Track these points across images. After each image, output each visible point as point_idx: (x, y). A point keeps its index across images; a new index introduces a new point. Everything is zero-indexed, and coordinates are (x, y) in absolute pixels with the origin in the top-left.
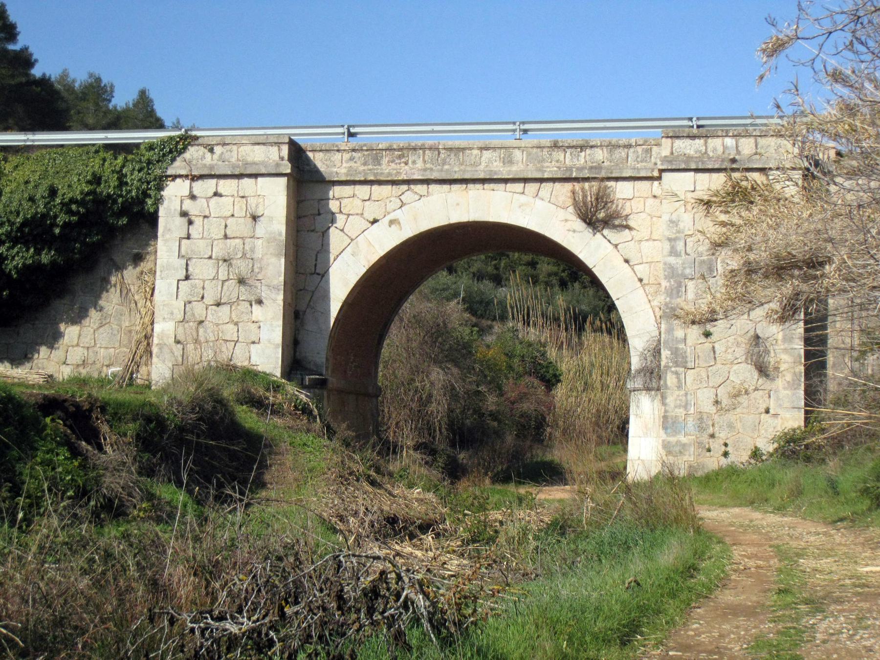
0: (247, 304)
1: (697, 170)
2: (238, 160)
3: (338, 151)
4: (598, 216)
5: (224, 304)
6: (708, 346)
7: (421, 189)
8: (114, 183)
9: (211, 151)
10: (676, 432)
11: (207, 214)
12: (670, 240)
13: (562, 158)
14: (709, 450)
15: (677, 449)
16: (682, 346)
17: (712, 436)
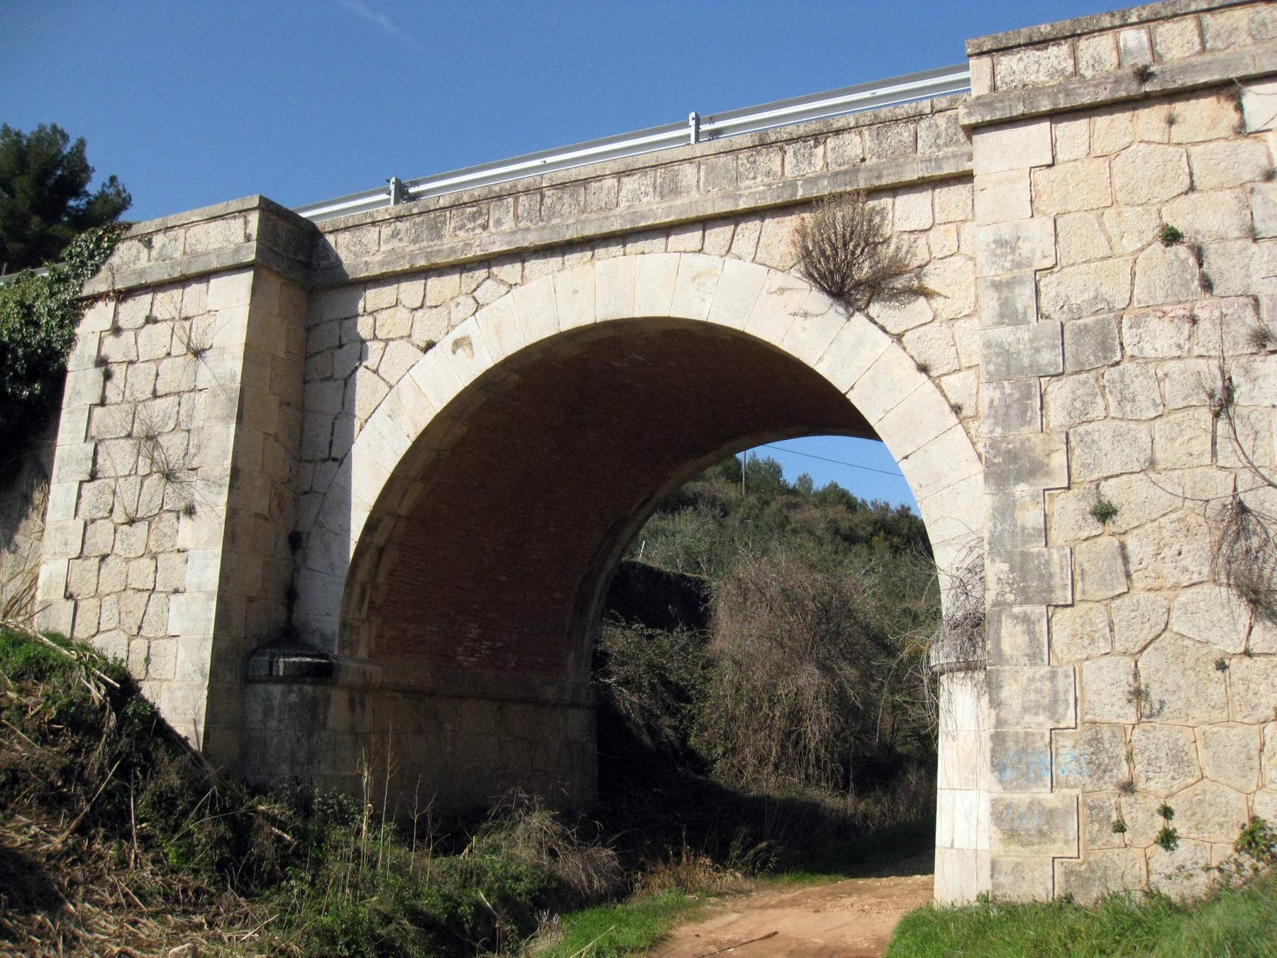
0: (173, 515)
1: (1056, 115)
2: (185, 253)
3: (373, 223)
4: (852, 274)
5: (142, 519)
6: (1108, 543)
7: (509, 271)
9: (149, 245)
10: (1028, 778)
11: (133, 357)
12: (997, 286)
13: (776, 166)
14: (1120, 828)
15: (1032, 824)
16: (1036, 547)
17: (1128, 788)
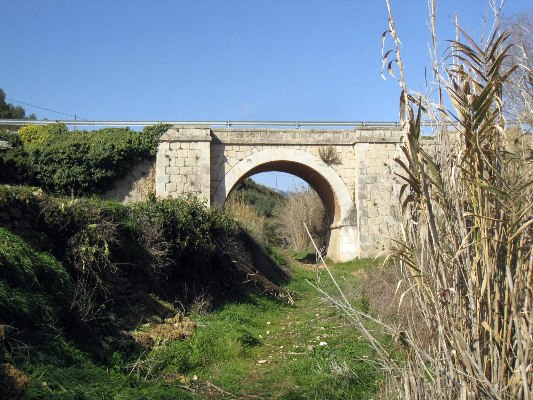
1: (370, 143)
4: (330, 159)
6: (375, 209)
7: (260, 147)
8: (137, 143)
9: (178, 131)
10: (365, 241)
12: (360, 169)
14: (377, 248)
15: (365, 248)
16: (366, 209)
17: (378, 243)
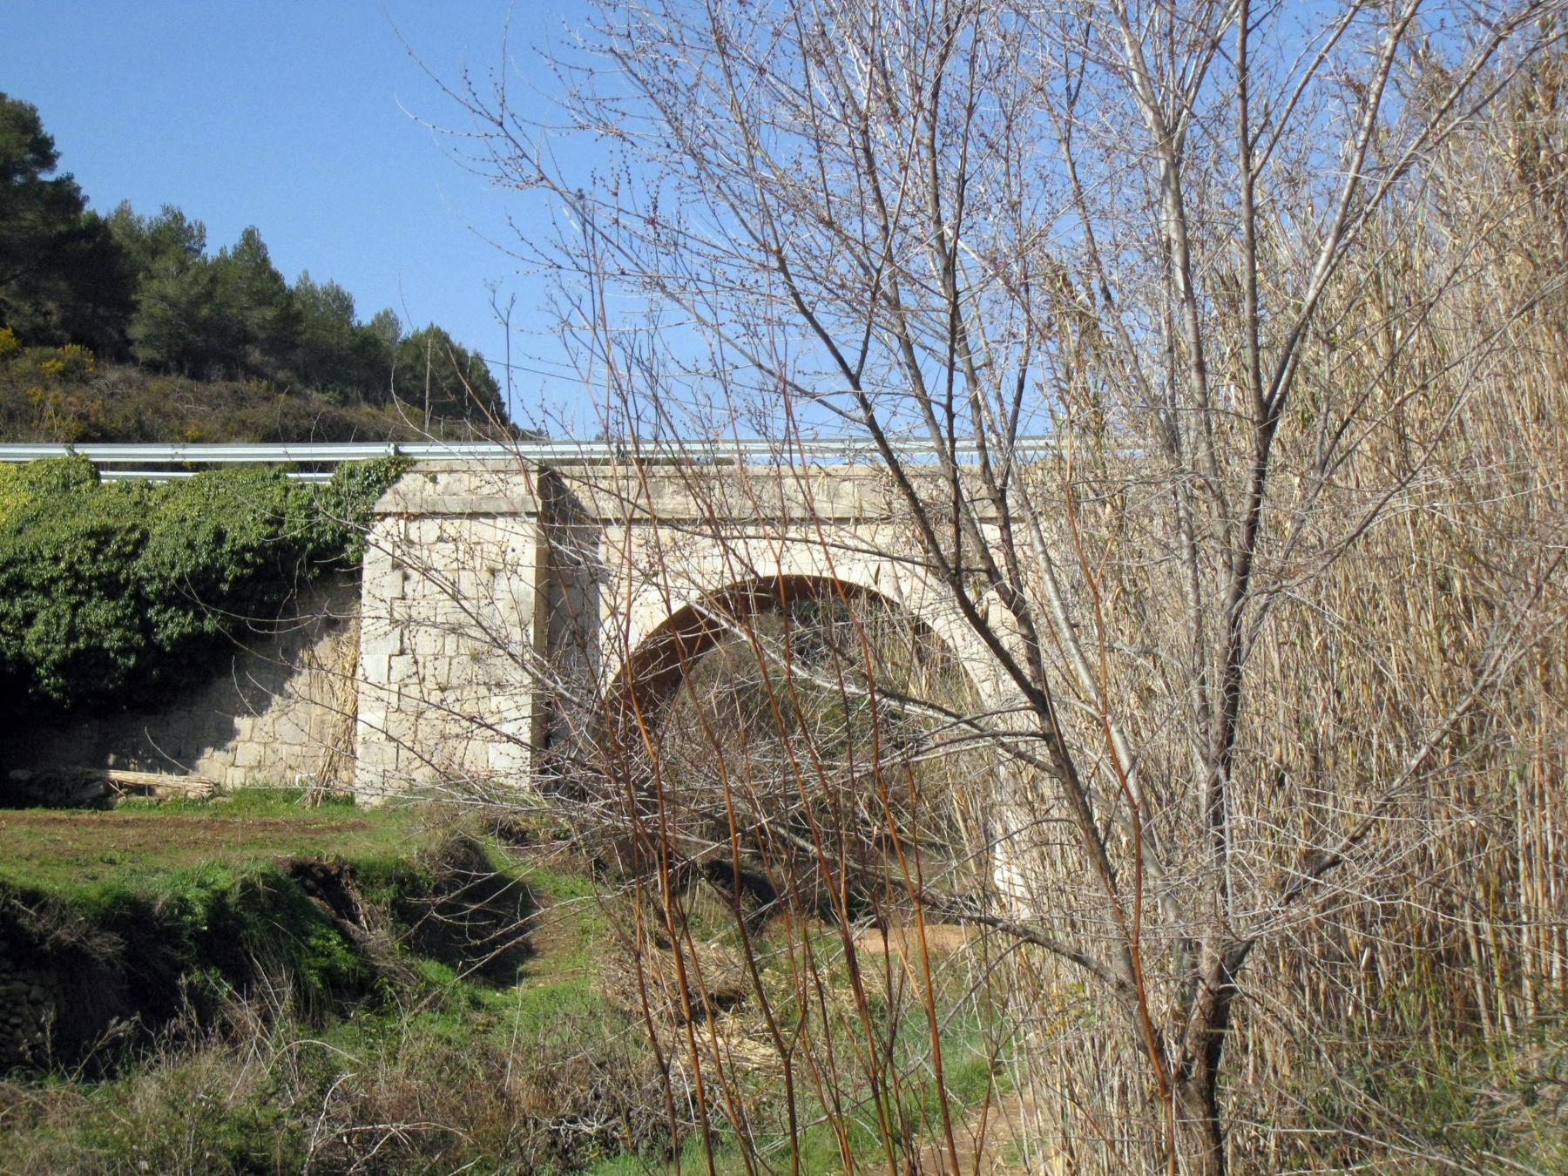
8: (301, 520)
9: (434, 480)
